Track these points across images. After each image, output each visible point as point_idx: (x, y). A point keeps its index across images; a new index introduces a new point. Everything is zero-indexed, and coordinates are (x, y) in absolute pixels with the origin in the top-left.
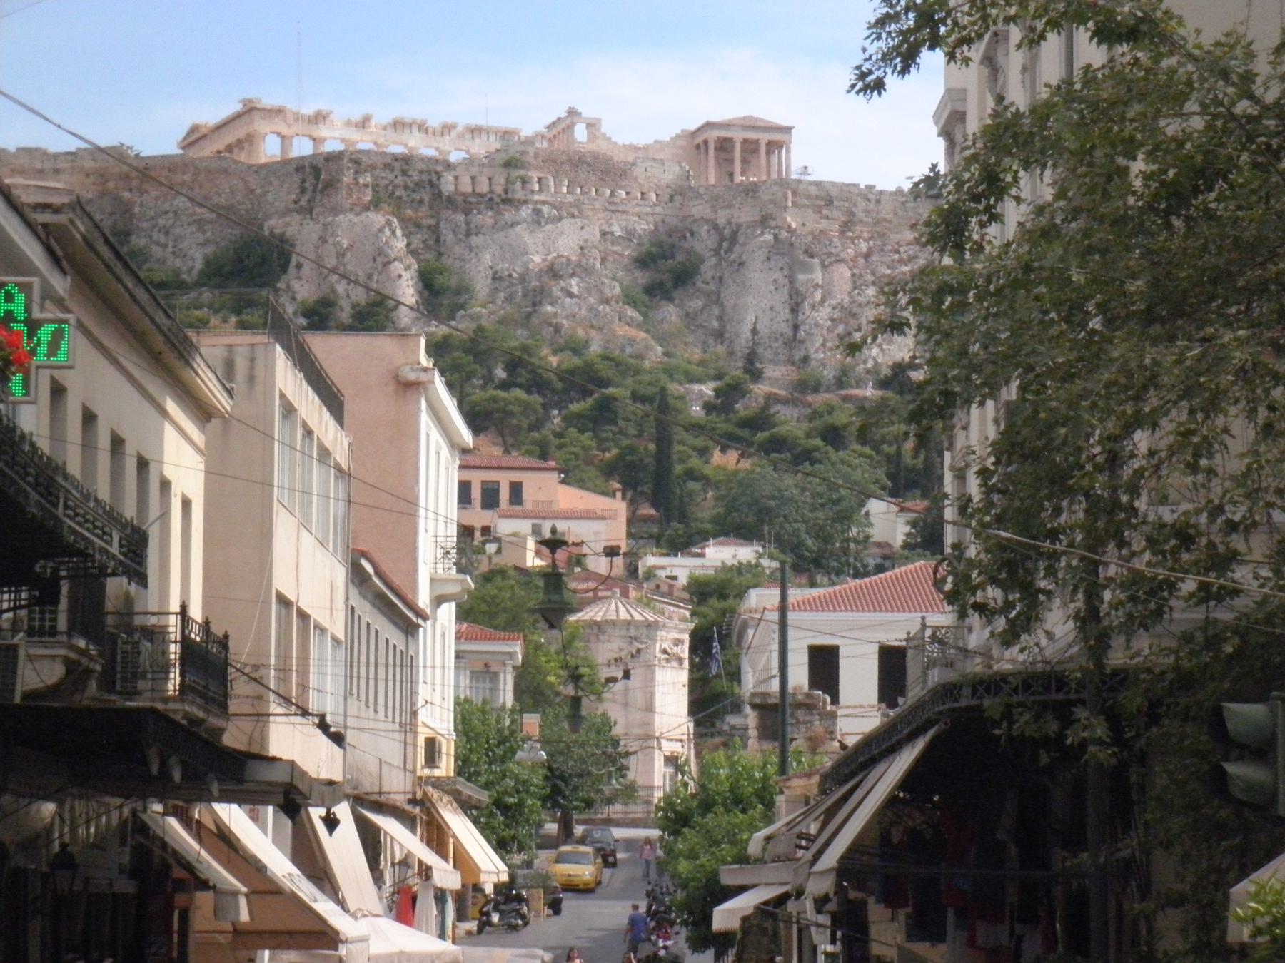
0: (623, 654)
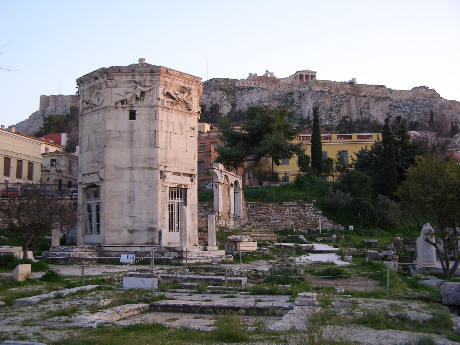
0: (128, 97)
